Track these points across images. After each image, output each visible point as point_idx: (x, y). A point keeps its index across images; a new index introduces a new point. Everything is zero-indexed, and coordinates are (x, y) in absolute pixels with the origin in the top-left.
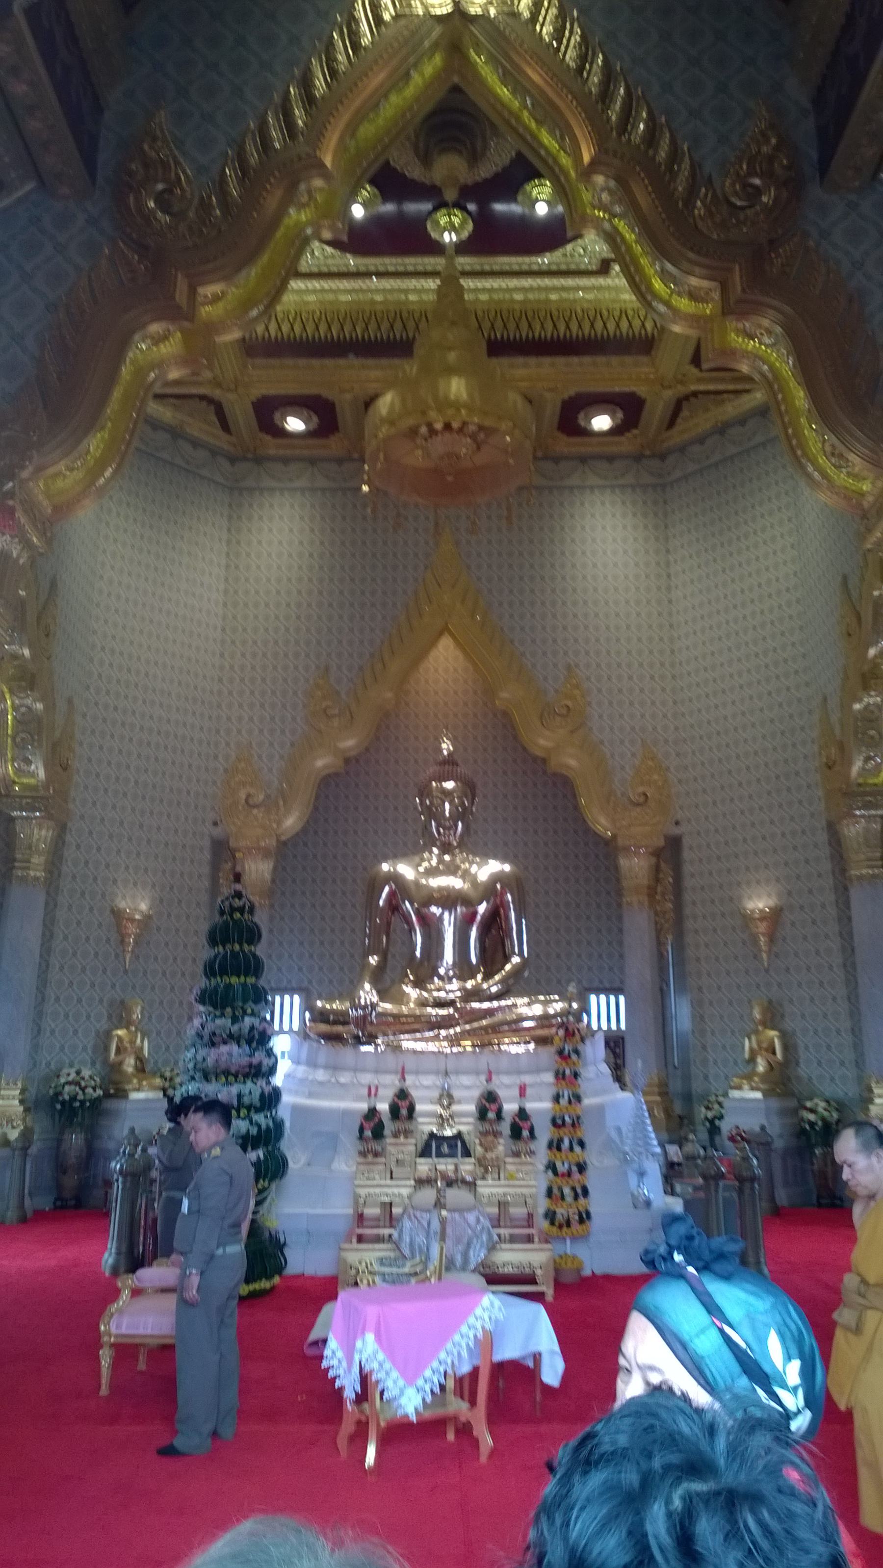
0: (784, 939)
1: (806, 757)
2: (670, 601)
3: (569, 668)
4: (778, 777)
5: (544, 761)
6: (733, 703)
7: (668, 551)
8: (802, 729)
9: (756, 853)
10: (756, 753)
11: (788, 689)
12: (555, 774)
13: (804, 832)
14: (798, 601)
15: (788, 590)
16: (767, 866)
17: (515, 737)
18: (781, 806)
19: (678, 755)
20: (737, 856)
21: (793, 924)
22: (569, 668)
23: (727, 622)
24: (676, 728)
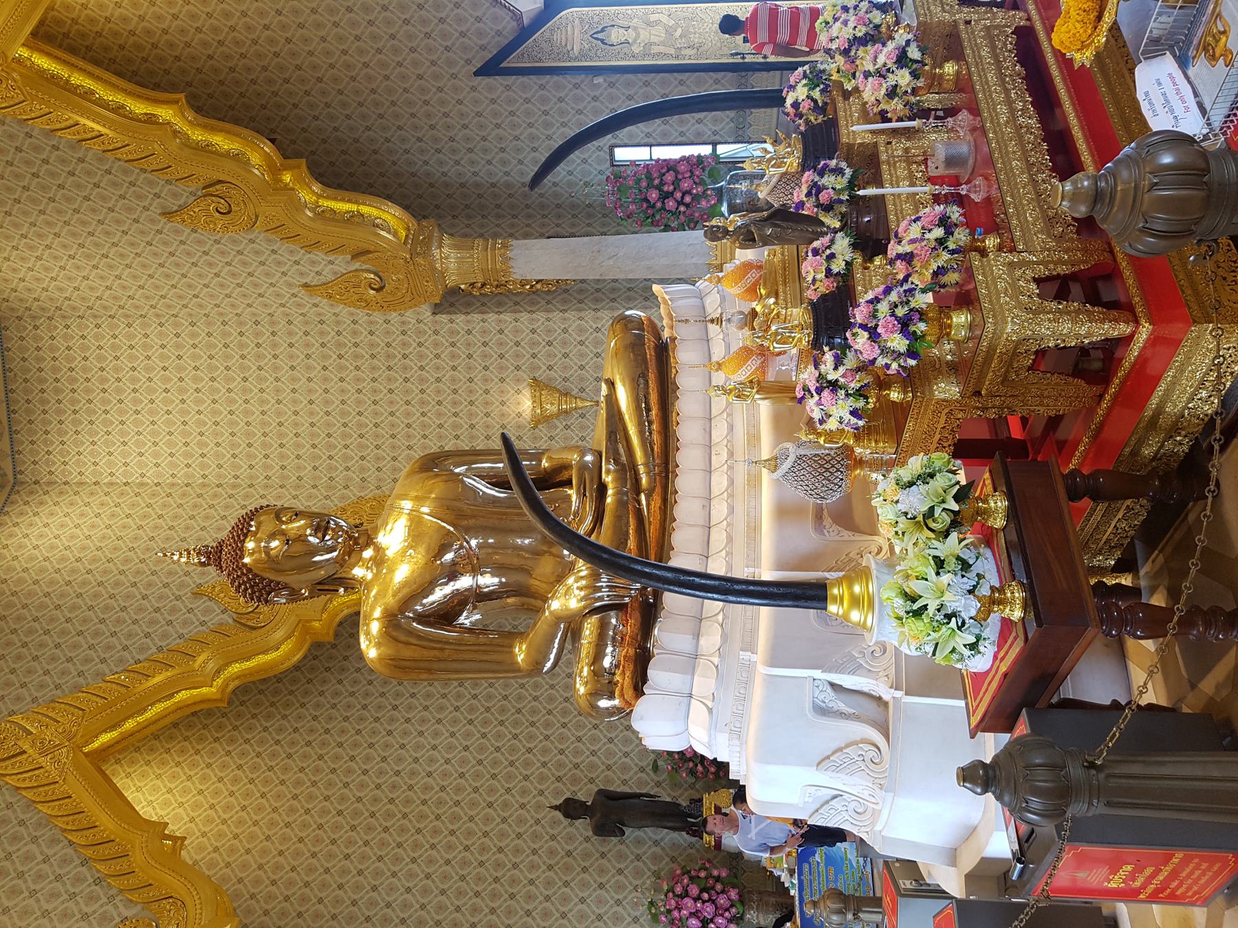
0: (565, 379)
1: (371, 333)
2: (158, 484)
3: (197, 595)
4: (389, 368)
5: (317, 645)
6: (296, 413)
7: (96, 483)
8: (339, 333)
9: (471, 403)
10: (359, 391)
11: (291, 345)
12: (337, 635)
13: (453, 345)
14: (193, 324)
15: (177, 335)
16: (487, 392)
17: (279, 678)
18: (422, 368)
19: (346, 487)
20: (472, 426)
21: (550, 368)
22: (197, 595)
23: (199, 412)
24: (314, 487)
